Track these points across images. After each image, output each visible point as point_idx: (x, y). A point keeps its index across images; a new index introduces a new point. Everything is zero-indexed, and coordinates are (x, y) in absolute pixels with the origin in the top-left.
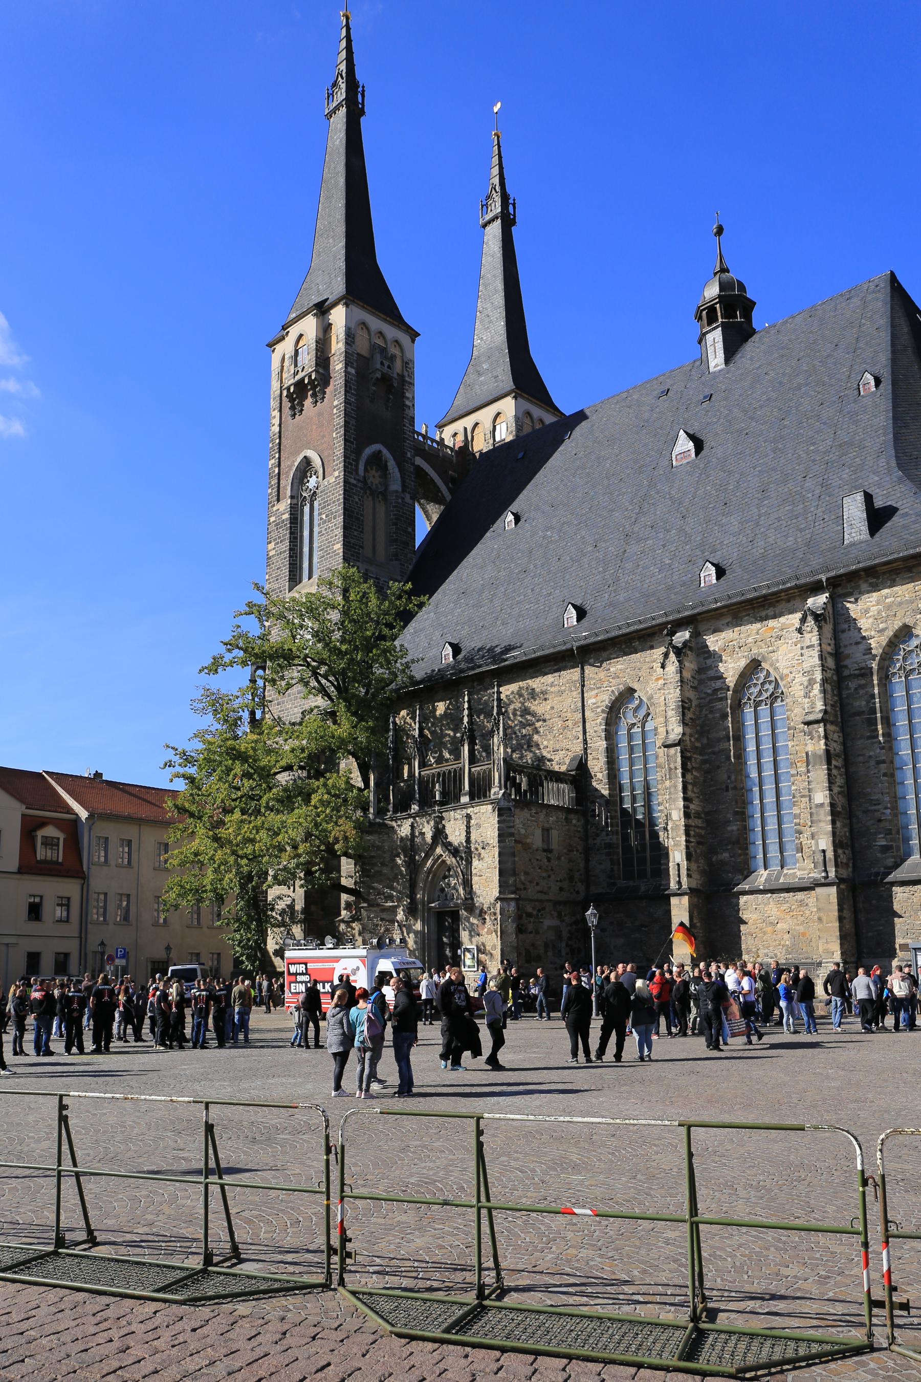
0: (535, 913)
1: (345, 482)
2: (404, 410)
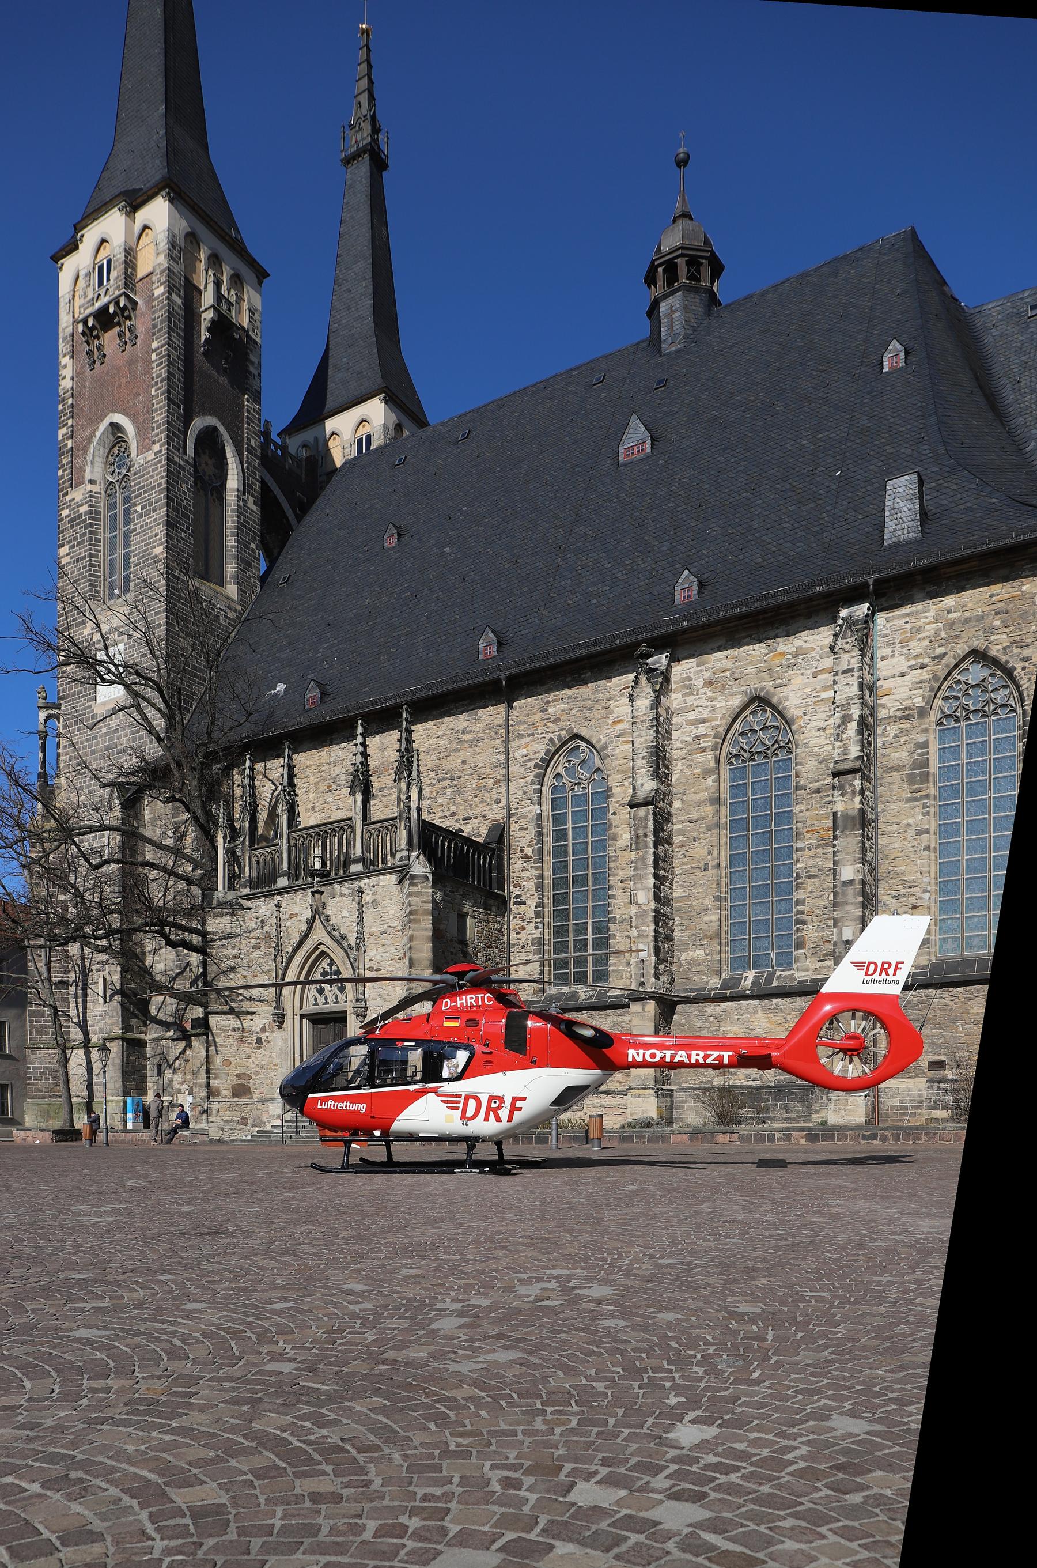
1: (168, 459)
2: (247, 378)
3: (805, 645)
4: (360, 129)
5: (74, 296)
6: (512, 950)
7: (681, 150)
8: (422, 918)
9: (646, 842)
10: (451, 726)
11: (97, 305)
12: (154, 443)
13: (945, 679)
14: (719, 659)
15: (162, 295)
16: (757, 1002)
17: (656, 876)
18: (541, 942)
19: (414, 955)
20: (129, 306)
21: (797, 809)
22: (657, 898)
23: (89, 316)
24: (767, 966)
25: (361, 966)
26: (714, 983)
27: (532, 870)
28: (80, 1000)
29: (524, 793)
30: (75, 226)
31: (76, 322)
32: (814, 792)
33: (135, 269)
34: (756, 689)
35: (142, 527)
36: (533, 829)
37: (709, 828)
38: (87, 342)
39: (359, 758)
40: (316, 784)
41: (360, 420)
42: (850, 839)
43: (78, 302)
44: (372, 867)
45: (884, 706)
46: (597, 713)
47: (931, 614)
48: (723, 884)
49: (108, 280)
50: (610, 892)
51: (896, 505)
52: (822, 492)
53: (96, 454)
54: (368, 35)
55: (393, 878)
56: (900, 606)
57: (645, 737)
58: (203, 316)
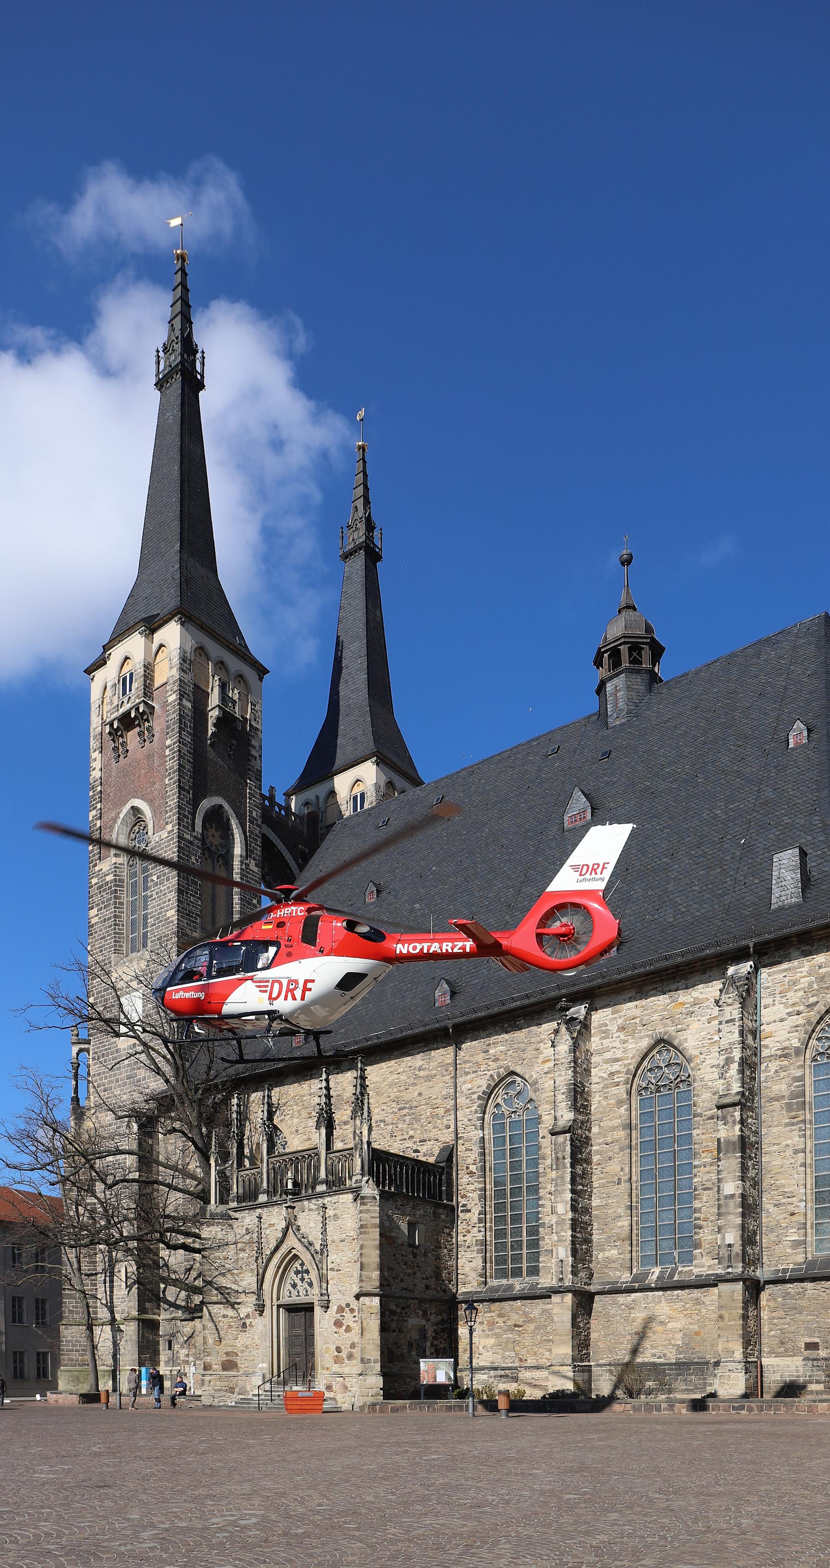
0: (398, 1311)
1: (179, 837)
2: (249, 760)
3: (701, 996)
4: (357, 529)
5: (103, 702)
6: (460, 1249)
7: (625, 552)
8: (371, 1230)
9: (564, 1164)
10: (410, 1064)
11: (121, 711)
12: (167, 823)
13: (818, 1023)
14: (630, 1009)
15: (175, 701)
16: (661, 1293)
17: (573, 1191)
18: (484, 1243)
19: (364, 1260)
20: (147, 711)
21: (695, 1132)
22: (574, 1208)
23: (115, 719)
24: (671, 1263)
25: (325, 1267)
26: (626, 1277)
27: (476, 1184)
28: (108, 1284)
29: (469, 1120)
30: (103, 647)
31: (103, 724)
32: (708, 1119)
33: (152, 680)
34: (660, 1033)
35: (157, 893)
36: (476, 1150)
37: (622, 1149)
38: (113, 740)
39: (324, 1099)
40: (299, 1111)
41: (355, 780)
42: (731, 1161)
43: (106, 708)
44: (336, 1184)
45: (767, 1047)
46: (530, 1053)
47: (805, 969)
48: (634, 1195)
49: (130, 690)
50: (540, 1203)
51: (781, 875)
52: (728, 858)
53: (120, 832)
54: (364, 450)
55: (350, 1197)
56: (780, 963)
57: (565, 1077)
58: (210, 714)
